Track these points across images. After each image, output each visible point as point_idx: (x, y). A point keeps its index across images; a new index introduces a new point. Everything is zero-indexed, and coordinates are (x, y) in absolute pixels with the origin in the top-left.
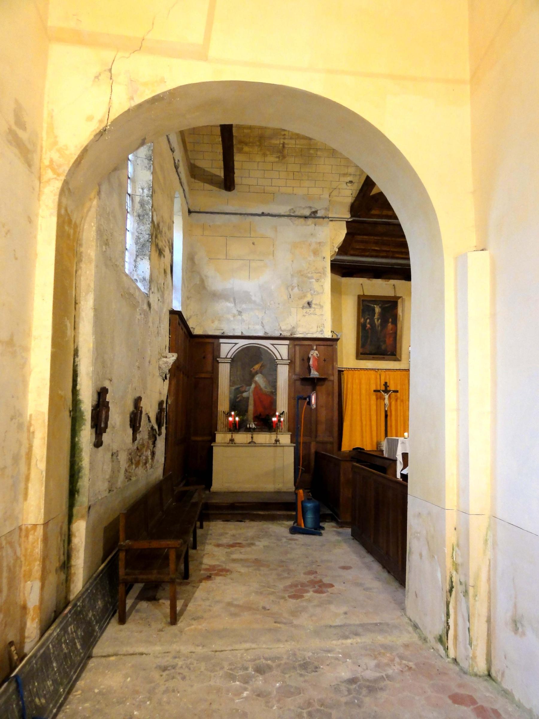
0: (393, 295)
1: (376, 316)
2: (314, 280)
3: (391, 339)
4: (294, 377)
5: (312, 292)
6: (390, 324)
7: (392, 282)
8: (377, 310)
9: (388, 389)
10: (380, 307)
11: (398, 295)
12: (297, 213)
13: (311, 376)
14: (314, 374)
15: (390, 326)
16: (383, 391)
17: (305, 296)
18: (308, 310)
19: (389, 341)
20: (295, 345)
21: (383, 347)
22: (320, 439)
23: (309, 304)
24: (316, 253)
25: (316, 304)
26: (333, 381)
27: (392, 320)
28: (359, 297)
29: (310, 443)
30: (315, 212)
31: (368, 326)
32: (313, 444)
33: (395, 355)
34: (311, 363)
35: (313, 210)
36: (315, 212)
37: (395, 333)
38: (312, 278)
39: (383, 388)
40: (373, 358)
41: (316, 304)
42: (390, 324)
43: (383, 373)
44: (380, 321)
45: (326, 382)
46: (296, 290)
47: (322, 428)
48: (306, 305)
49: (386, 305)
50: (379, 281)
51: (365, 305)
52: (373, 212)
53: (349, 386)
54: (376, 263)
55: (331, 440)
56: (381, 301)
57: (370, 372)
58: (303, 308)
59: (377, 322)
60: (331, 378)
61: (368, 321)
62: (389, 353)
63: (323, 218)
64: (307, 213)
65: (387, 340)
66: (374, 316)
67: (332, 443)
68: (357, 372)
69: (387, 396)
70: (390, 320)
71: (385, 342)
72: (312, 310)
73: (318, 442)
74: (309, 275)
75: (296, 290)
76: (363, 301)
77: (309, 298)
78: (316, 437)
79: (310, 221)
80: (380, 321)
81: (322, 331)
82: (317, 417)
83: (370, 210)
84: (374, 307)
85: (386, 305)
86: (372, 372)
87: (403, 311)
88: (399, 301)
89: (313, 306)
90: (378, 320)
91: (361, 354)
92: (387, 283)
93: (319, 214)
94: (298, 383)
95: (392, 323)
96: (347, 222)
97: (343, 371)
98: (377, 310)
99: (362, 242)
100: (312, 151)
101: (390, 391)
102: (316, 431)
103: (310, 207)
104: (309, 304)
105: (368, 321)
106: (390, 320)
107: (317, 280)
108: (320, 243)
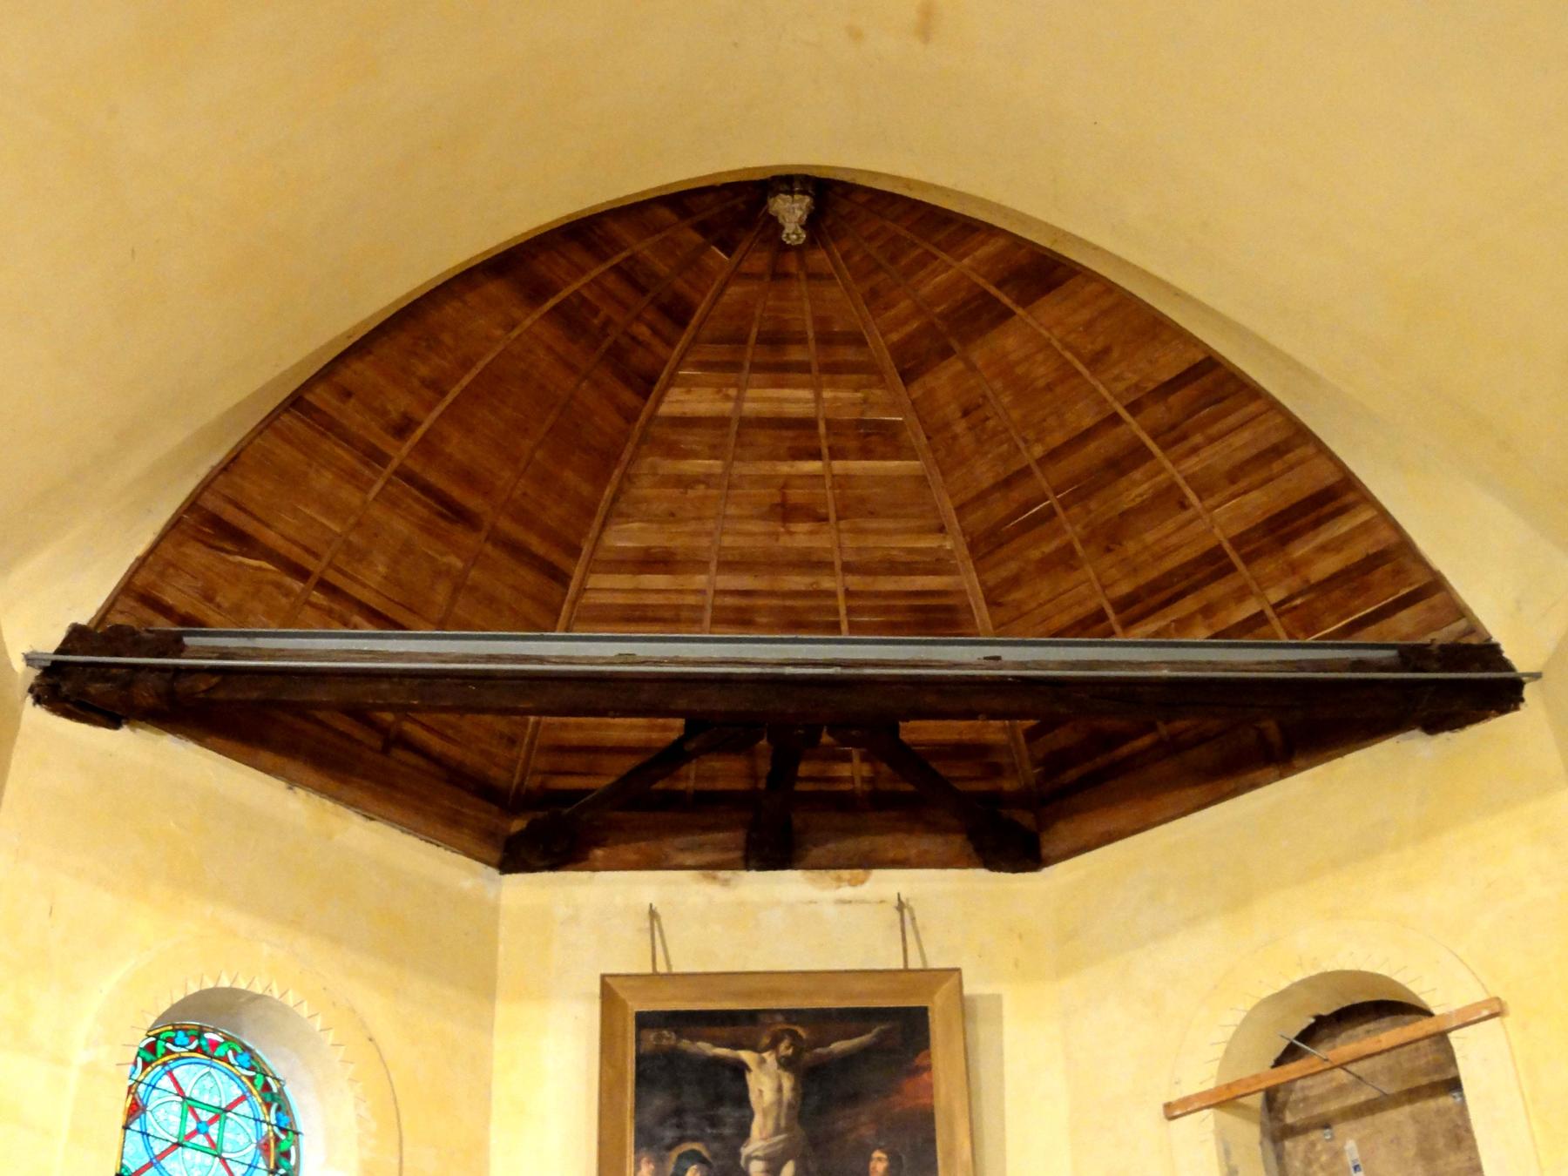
1: (760, 1137)
7: (888, 883)
8: (767, 1084)
10: (786, 1064)
11: (935, 963)
28: (610, 992)
49: (838, 1046)
52: (681, 401)
56: (792, 1015)
66: (744, 1133)
76: (645, 1021)
83: (646, 383)
84: (740, 1069)
85: (838, 1046)
92: (847, 892)
98: (767, 1084)
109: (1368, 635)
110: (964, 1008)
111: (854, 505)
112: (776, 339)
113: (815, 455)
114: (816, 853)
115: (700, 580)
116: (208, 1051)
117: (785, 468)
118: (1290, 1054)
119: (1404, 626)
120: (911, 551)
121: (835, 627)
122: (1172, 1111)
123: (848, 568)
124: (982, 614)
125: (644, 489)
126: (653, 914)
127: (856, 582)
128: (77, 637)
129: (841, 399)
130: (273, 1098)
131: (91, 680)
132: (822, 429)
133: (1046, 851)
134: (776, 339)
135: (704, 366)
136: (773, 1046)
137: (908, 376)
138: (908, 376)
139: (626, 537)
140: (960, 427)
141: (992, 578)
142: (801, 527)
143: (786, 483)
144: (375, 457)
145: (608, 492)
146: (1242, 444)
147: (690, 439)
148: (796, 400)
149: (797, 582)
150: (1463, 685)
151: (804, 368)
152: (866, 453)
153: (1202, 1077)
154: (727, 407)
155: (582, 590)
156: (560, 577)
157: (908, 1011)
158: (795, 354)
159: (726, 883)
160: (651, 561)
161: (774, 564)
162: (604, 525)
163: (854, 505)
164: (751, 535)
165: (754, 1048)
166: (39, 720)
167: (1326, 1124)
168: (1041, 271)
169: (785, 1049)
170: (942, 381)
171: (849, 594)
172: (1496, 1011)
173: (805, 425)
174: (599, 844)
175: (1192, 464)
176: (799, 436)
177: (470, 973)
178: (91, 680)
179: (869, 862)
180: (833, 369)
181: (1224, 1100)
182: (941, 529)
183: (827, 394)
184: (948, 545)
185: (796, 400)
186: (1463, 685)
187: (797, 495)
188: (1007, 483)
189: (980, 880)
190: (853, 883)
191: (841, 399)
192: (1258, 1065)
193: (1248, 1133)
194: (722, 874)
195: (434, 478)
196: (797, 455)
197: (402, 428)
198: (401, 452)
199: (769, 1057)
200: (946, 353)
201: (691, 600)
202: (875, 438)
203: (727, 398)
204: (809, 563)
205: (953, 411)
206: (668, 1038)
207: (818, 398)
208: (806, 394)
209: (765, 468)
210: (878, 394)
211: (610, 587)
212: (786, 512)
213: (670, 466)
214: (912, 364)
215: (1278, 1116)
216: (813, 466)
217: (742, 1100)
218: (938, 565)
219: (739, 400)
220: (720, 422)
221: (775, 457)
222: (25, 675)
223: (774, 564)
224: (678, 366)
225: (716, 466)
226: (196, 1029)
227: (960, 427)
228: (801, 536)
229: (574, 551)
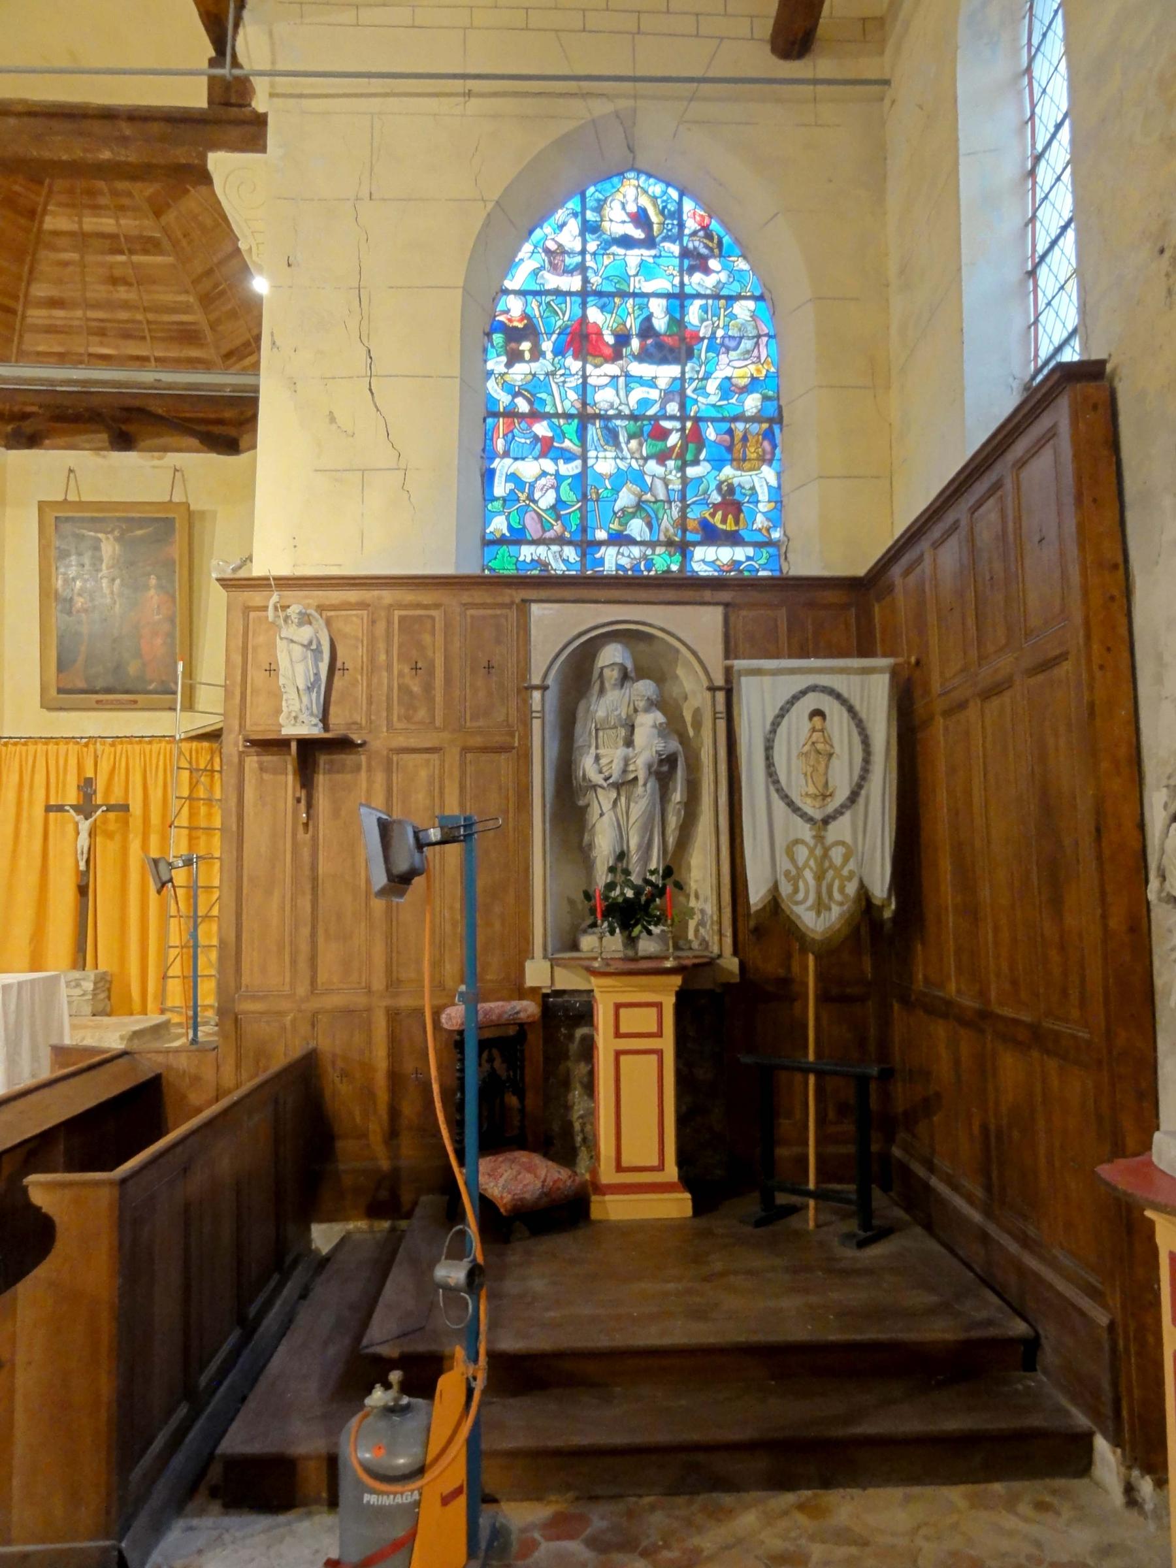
6: (152, 592)
10: (117, 539)
16: (77, 809)
21: (132, 669)
27: (158, 578)
28: (42, 506)
39: (72, 797)
40: (98, 702)
42: (152, 592)
43: (107, 749)
44: (118, 581)
50: (130, 458)
56: (119, 519)
62: (152, 687)
68: (18, 747)
80: (118, 581)
83: (32, 214)
91: (60, 691)
92: (156, 462)
95: (160, 587)
99: (51, 330)
101: (99, 806)
106: (153, 581)
111: (143, 279)
113: (121, 252)
114: (142, 444)
115: (79, 313)
120: (175, 302)
121: (143, 338)
123: (145, 309)
124: (209, 336)
125: (44, 267)
126: (71, 471)
127: (151, 316)
132: (123, 239)
135: (60, 205)
136: (112, 532)
137: (158, 214)
138: (158, 214)
139: (40, 290)
140: (184, 243)
141: (213, 317)
142: (122, 289)
143: (111, 266)
145: (26, 268)
147: (62, 242)
148: (107, 224)
149: (123, 315)
151: (106, 207)
152: (146, 252)
154: (74, 227)
155: (24, 317)
156: (12, 311)
159: (104, 457)
160: (55, 303)
161: (109, 305)
162: (29, 284)
163: (143, 279)
164: (99, 291)
165: (106, 533)
169: (116, 533)
170: (170, 217)
171: (148, 322)
173: (113, 237)
174: (47, 437)
176: (114, 243)
179: (165, 449)
180: (122, 208)
182: (187, 292)
183: (122, 222)
184: (191, 300)
185: (107, 224)
187: (117, 273)
190: (160, 458)
194: (102, 453)
199: (110, 536)
200: (169, 206)
201: (76, 323)
202: (150, 245)
203: (73, 222)
204: (126, 305)
205: (179, 234)
207: (118, 224)
208: (112, 221)
209: (100, 258)
210: (146, 222)
211: (37, 315)
212: (114, 281)
213: (53, 256)
216: (122, 258)
218: (187, 309)
219: (80, 223)
220: (71, 234)
221: (103, 253)
223: (109, 305)
224: (46, 204)
225: (75, 256)
227: (184, 243)
228: (122, 293)
229: (16, 298)
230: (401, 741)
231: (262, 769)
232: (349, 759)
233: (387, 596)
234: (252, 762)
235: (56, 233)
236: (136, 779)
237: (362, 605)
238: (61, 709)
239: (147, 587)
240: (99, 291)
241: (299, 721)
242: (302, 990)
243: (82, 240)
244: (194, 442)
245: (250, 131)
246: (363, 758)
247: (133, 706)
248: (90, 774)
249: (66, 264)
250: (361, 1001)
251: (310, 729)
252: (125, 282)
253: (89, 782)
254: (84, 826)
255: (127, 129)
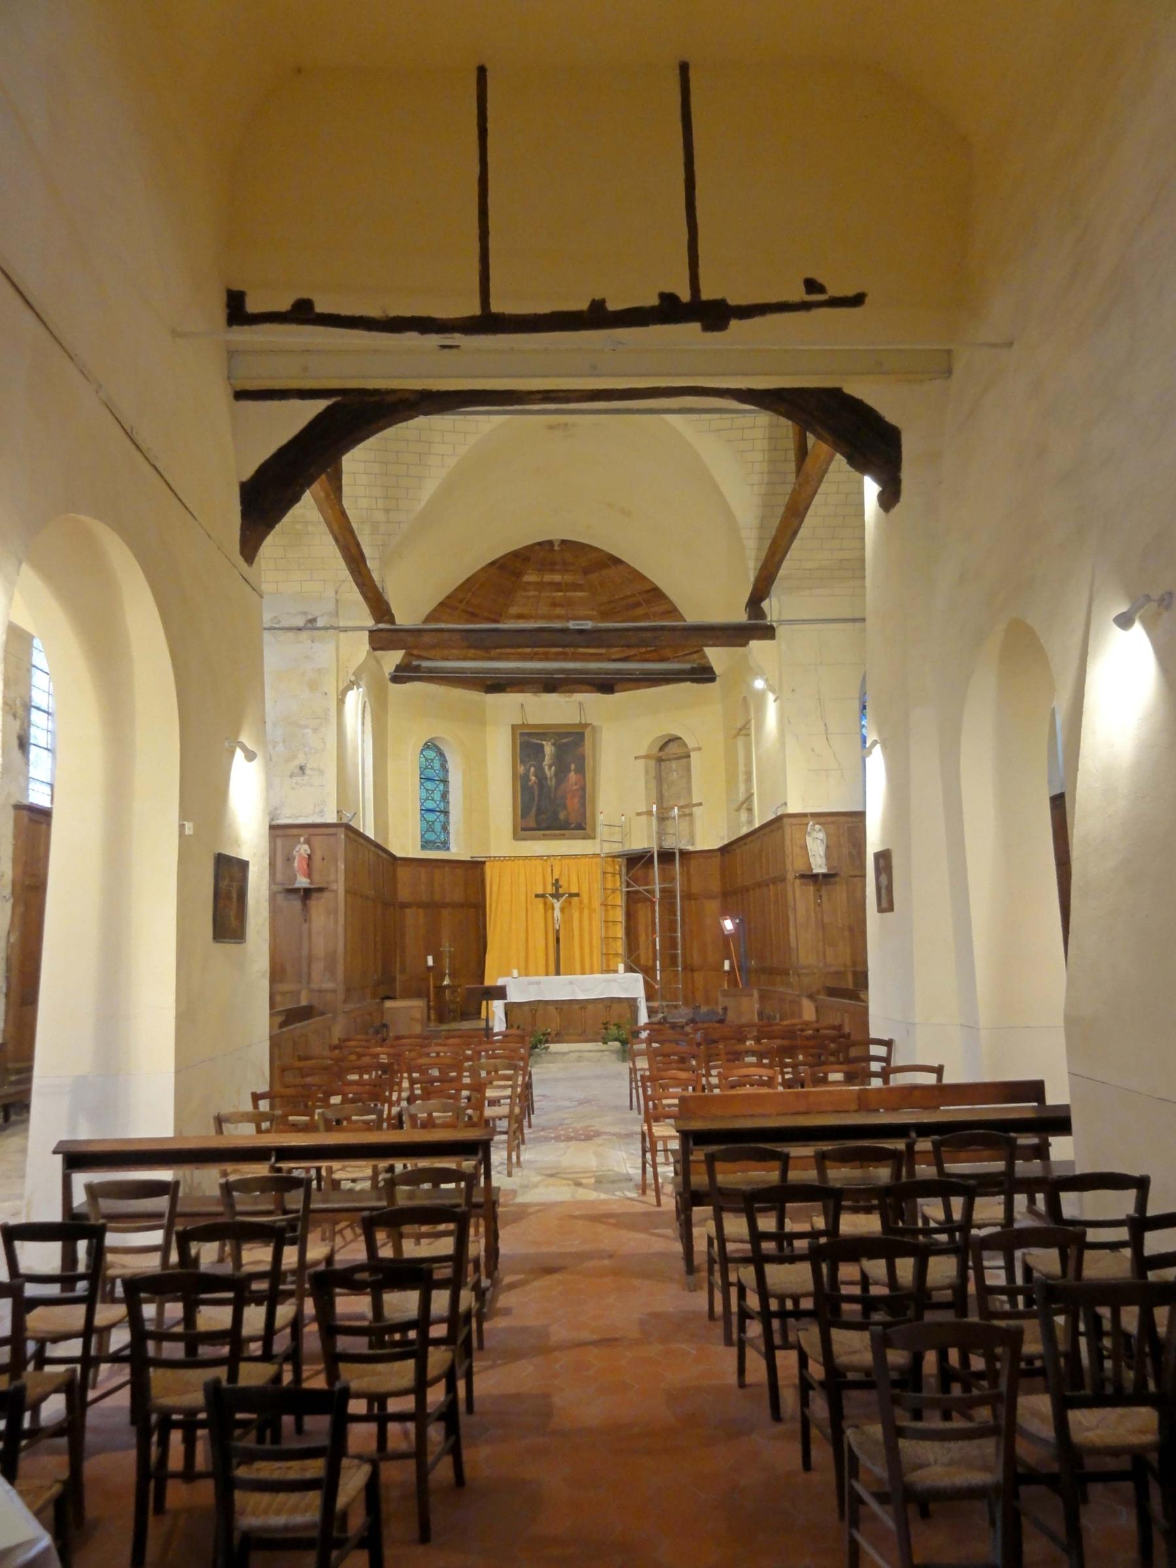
0: (577, 722)
2: (309, 731)
3: (576, 800)
4: (275, 888)
5: (307, 749)
6: (572, 773)
8: (549, 749)
9: (561, 891)
10: (553, 744)
12: (284, 624)
13: (297, 885)
14: (302, 882)
15: (573, 776)
16: (552, 895)
17: (294, 757)
18: (299, 779)
19: (573, 803)
20: (277, 836)
21: (562, 816)
22: (314, 986)
23: (302, 768)
24: (313, 686)
25: (312, 769)
26: (336, 891)
28: (514, 727)
29: (299, 992)
30: (314, 620)
31: (533, 778)
32: (304, 993)
33: (584, 829)
34: (296, 864)
35: (310, 617)
36: (314, 620)
37: (583, 789)
38: (306, 727)
39: (550, 889)
41: (312, 769)
42: (572, 773)
45: (326, 895)
46: (280, 748)
47: (318, 967)
48: (297, 771)
51: (528, 743)
53: (495, 888)
54: (524, 671)
55: (329, 985)
57: (533, 862)
58: (291, 776)
59: (549, 772)
60: (334, 887)
61: (532, 769)
63: (326, 628)
64: (300, 622)
65: (568, 802)
66: (543, 760)
67: (334, 991)
69: (558, 905)
70: (573, 766)
71: (565, 807)
72: (306, 778)
73: (312, 991)
74: (302, 723)
75: (280, 748)
76: (521, 734)
77: (300, 760)
78: (309, 982)
79: (304, 635)
81: (322, 811)
82: (310, 950)
83: (518, 574)
84: (542, 746)
86: (538, 862)
87: (594, 745)
88: (588, 733)
89: (308, 771)
90: (550, 768)
91: (523, 829)
93: (320, 624)
94: (280, 897)
95: (576, 771)
96: (370, 631)
97: (484, 863)
98: (549, 749)
100: (298, 527)
102: (309, 974)
103: (305, 613)
104: (302, 768)
105: (532, 769)
107: (315, 730)
108: (319, 670)
109: (688, 657)
110: (594, 728)
112: (553, 564)
116: (428, 747)
117: (555, 594)
118: (661, 749)
119: (695, 656)
122: (636, 758)
128: (398, 668)
129: (568, 578)
130: (441, 754)
131: (402, 675)
133: (616, 688)
134: (553, 564)
139: (513, 610)
144: (457, 608)
146: (663, 608)
148: (557, 578)
150: (704, 674)
152: (575, 591)
153: (643, 752)
157: (578, 733)
158: (558, 567)
166: (393, 687)
167: (669, 760)
168: (617, 561)
170: (594, 577)
172: (699, 749)
173: (558, 584)
175: (653, 610)
176: (558, 586)
177: (479, 720)
178: (402, 675)
181: (647, 757)
185: (557, 578)
186: (704, 674)
188: (609, 602)
189: (599, 696)
191: (568, 578)
192: (655, 751)
193: (652, 763)
195: (470, 609)
196: (557, 591)
197: (461, 602)
198: (462, 606)
202: (576, 587)
206: (526, 738)
212: (555, 605)
214: (586, 572)
215: (660, 760)
216: (561, 594)
217: (543, 751)
220: (538, 583)
222: (388, 677)
225: (536, 593)
226: (427, 746)
230: (852, 873)
231: (802, 884)
232: (833, 880)
233: (842, 819)
234: (798, 882)
235: (529, 583)
236: (574, 878)
237: (833, 823)
238: (524, 839)
239: (569, 771)
240: (544, 609)
241: (819, 866)
242: (821, 965)
243: (540, 586)
244: (589, 688)
245: (768, 632)
246: (837, 879)
247: (562, 837)
248: (556, 876)
249: (528, 598)
250: (842, 969)
251: (824, 870)
252: (561, 606)
253: (557, 881)
254: (558, 905)
255: (719, 633)
